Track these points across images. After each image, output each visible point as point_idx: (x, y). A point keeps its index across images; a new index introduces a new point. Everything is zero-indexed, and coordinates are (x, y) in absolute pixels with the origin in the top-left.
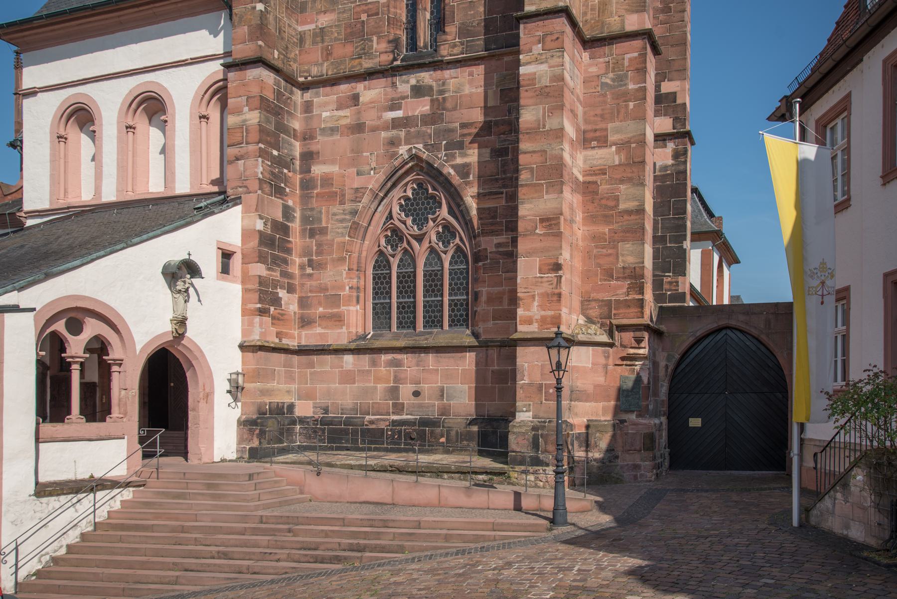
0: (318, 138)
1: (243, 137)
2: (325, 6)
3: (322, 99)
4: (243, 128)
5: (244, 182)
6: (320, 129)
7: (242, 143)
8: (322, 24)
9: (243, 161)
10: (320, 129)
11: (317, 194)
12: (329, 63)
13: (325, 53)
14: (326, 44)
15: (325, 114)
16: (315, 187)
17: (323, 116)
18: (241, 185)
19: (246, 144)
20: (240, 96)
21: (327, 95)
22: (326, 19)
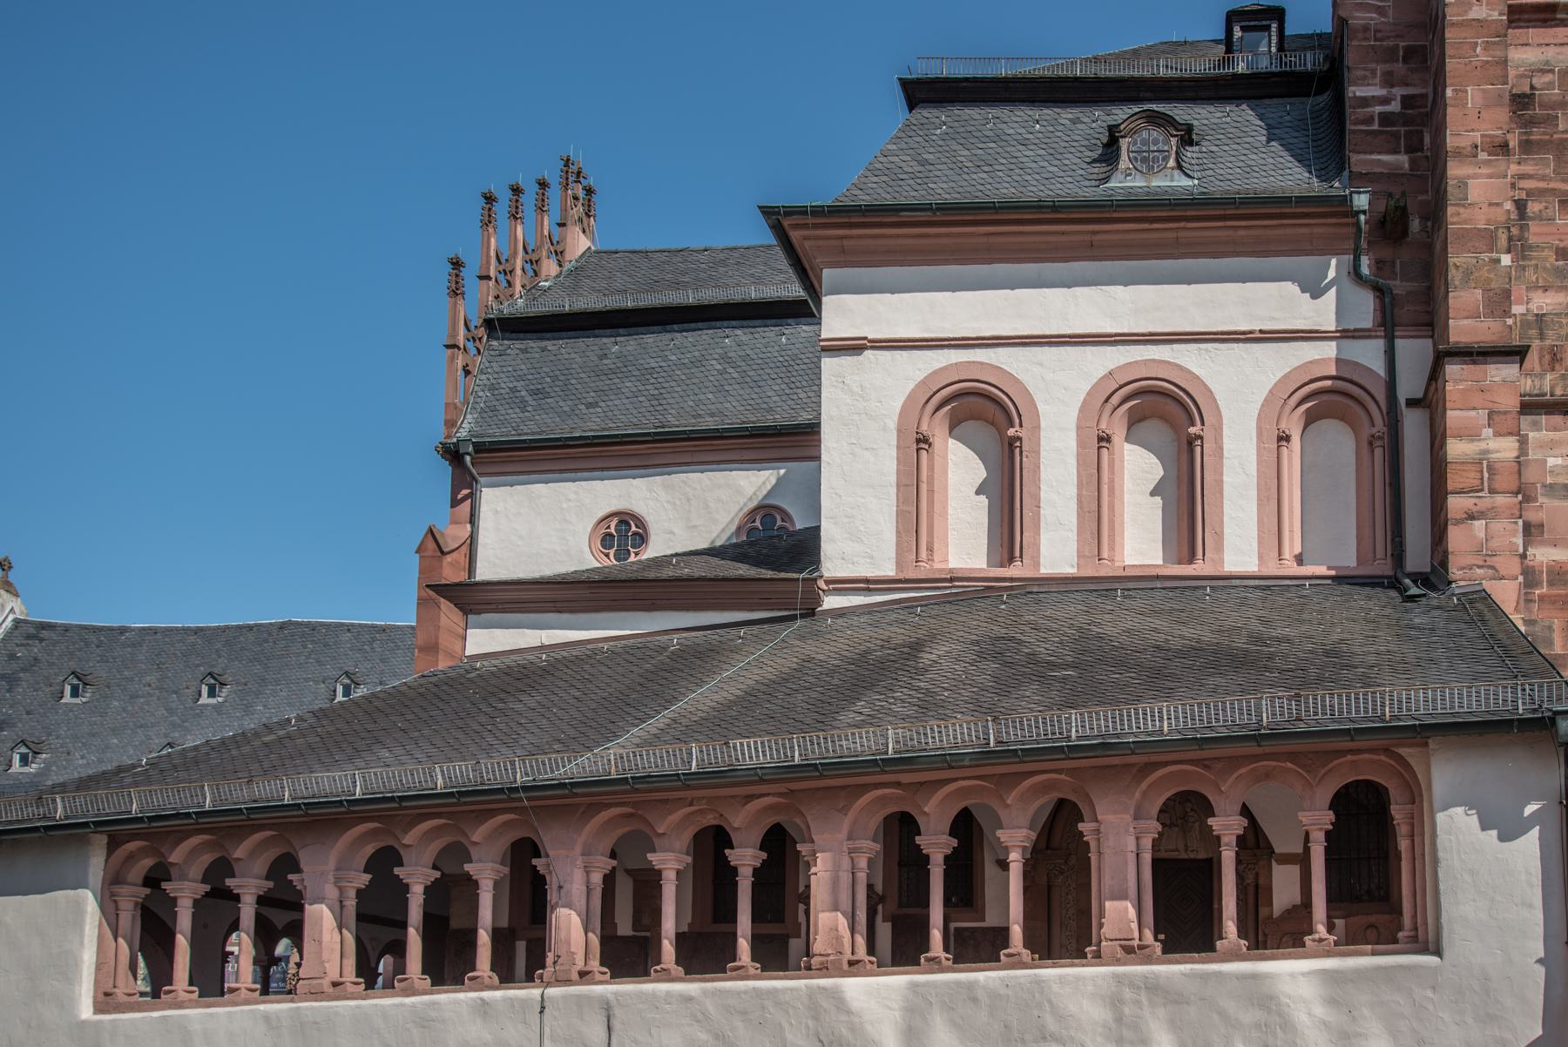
0: (1541, 499)
1: (1482, 479)
2: (1544, 279)
3: (1545, 435)
4: (1482, 464)
5: (1488, 558)
6: (1544, 486)
7: (1482, 490)
8: (1540, 308)
9: (1484, 522)
10: (1544, 486)
11: (1542, 598)
12: (1555, 375)
13: (1547, 357)
14: (1548, 342)
15: (1551, 462)
16: (1538, 584)
17: (1549, 465)
18: (1481, 563)
19: (1490, 493)
20: (1474, 409)
21: (1556, 429)
22: (1548, 301)
